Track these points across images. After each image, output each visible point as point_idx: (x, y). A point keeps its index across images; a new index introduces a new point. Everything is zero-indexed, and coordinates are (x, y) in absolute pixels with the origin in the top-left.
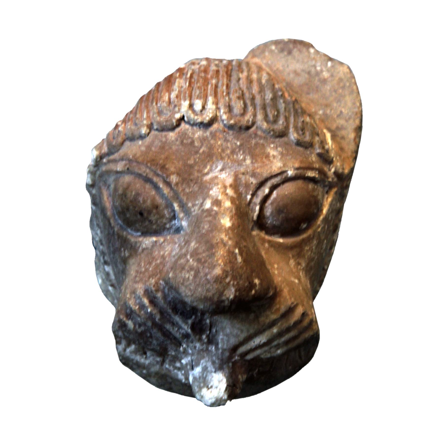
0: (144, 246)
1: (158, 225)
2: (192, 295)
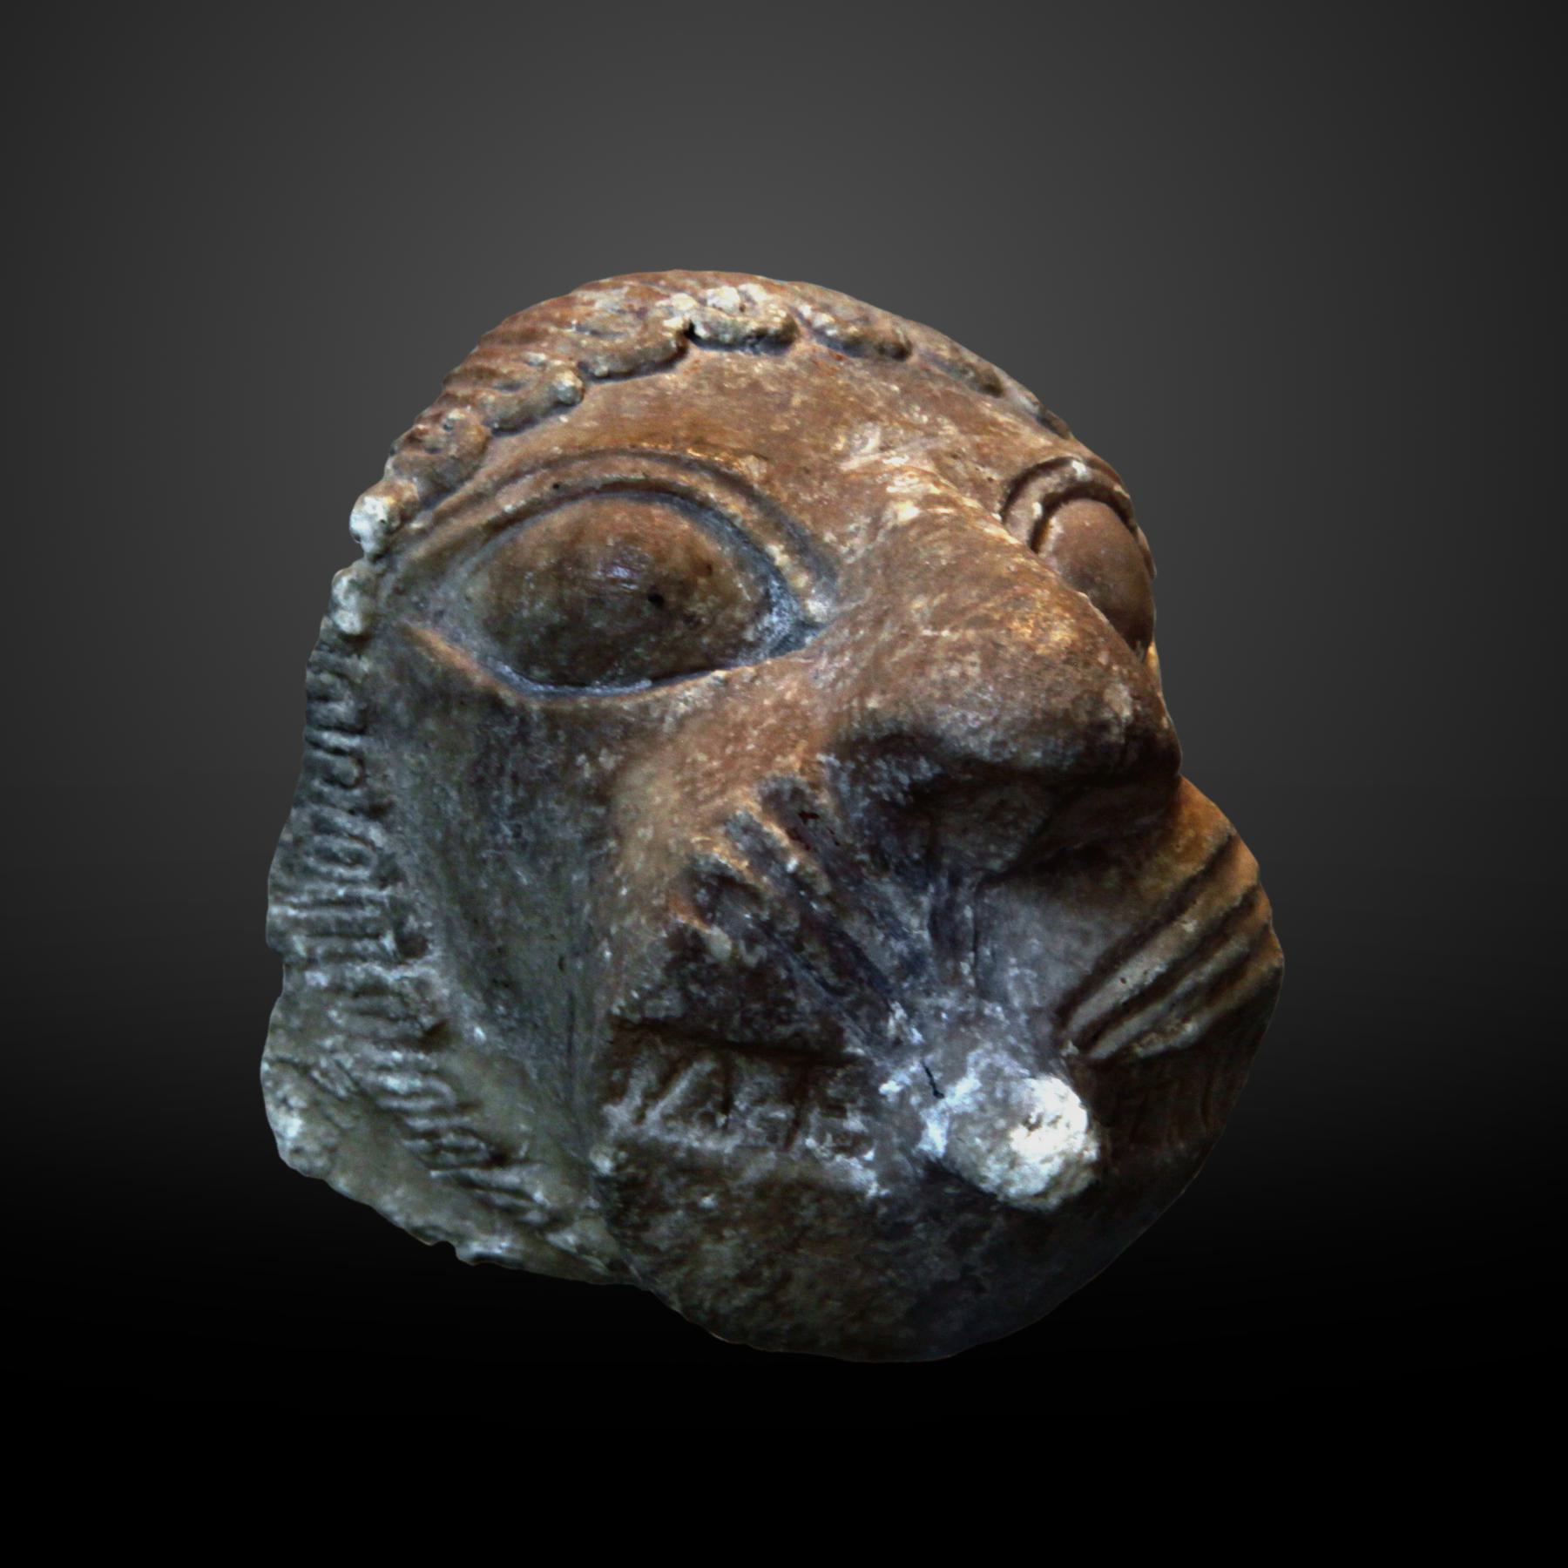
0: (682, 708)
1: (720, 635)
2: (996, 721)
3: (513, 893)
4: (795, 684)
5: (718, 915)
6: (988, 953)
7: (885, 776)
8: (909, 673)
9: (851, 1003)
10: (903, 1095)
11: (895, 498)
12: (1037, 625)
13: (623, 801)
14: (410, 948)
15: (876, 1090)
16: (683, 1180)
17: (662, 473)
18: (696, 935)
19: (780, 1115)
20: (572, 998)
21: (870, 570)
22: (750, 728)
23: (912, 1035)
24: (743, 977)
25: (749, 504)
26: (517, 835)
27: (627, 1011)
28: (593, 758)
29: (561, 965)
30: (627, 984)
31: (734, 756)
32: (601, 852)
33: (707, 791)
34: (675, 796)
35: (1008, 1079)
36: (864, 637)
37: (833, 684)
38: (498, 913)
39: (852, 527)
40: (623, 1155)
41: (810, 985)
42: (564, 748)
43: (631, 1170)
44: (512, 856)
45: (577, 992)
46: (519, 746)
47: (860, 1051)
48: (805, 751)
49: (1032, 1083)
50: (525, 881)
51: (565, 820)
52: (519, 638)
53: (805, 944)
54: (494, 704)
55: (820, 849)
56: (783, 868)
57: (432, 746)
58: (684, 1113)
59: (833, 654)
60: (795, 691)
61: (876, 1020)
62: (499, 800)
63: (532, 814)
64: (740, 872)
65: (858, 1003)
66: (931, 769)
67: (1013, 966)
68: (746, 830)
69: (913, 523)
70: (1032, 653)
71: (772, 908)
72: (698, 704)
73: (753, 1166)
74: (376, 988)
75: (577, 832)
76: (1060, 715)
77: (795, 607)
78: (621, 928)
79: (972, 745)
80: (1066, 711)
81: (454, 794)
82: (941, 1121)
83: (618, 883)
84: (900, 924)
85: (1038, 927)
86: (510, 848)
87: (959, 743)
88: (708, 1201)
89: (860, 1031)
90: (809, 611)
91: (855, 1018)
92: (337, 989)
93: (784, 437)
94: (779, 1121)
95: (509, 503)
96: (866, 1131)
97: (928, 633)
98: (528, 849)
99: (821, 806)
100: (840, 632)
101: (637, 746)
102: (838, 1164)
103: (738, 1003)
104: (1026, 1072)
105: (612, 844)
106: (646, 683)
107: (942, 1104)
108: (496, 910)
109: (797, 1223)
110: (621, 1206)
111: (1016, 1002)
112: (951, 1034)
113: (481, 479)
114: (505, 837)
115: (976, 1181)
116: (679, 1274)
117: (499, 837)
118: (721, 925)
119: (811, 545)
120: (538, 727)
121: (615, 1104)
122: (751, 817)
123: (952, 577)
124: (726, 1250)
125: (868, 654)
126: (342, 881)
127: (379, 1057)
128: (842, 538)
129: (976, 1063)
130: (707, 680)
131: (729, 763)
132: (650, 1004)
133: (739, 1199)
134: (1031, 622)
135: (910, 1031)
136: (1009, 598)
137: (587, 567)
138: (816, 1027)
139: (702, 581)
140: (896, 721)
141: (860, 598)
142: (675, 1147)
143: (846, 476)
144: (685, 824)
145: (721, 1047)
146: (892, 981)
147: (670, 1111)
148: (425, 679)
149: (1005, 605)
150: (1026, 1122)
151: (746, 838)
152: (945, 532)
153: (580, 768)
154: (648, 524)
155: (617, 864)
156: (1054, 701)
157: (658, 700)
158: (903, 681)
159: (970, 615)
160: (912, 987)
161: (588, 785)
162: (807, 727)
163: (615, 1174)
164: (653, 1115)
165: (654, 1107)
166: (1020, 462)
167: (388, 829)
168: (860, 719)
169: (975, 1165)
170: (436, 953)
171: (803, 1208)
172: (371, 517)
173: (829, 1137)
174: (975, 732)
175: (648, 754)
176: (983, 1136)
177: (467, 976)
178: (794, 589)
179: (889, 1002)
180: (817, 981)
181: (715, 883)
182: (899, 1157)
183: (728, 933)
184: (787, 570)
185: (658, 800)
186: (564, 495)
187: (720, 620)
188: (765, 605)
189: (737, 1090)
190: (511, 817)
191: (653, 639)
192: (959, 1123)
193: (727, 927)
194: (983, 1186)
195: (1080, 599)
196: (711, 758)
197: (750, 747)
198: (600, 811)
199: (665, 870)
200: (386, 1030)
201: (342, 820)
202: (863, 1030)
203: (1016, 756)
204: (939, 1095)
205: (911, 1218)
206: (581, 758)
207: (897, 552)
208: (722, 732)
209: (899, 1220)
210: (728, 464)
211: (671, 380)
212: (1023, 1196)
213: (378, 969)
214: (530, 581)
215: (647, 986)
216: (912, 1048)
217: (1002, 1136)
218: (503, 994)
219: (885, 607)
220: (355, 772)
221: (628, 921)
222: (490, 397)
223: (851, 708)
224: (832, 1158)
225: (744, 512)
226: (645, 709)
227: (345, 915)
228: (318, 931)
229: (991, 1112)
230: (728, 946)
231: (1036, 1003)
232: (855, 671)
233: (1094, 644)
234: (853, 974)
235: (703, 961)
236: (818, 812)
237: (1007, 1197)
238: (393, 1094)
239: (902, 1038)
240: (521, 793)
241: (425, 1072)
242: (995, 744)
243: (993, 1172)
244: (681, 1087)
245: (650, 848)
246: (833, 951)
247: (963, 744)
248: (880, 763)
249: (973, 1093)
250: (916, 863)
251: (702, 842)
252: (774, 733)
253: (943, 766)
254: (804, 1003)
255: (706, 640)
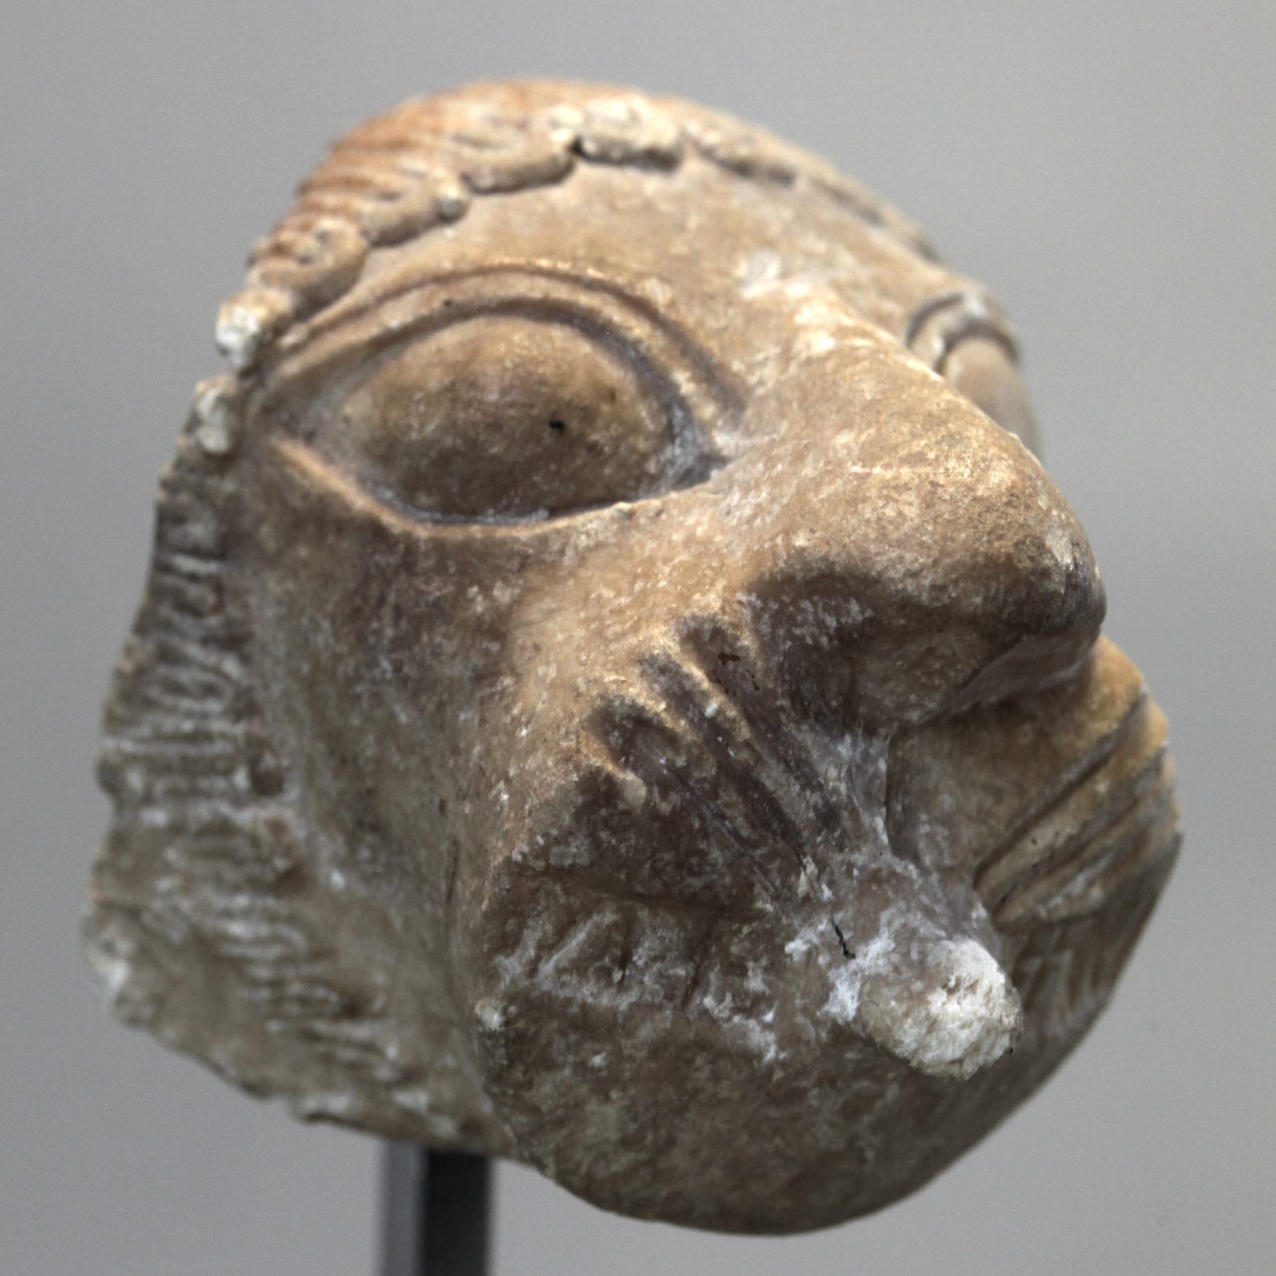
0: (583, 541)
1: (621, 466)
2: (935, 563)
3: (390, 731)
4: (705, 519)
5: (632, 759)
6: (899, 808)
7: (811, 618)
8: (841, 510)
9: (762, 856)
10: (810, 955)
11: (805, 328)
12: (975, 464)
13: (521, 638)
14: (266, 786)
15: (782, 947)
16: (573, 1037)
17: (561, 293)
18: (609, 779)
19: (681, 972)
20: (455, 843)
21: (783, 403)
22: (660, 564)
23: (822, 891)
24: (656, 825)
25: (654, 328)
26: (398, 669)
27: (530, 858)
28: (486, 591)
29: (442, 807)
30: (530, 829)
31: (643, 591)
32: (494, 690)
33: (618, 628)
34: (580, 633)
35: (924, 940)
36: (783, 472)
37: (750, 520)
38: (369, 752)
39: (760, 357)
40: (513, 1009)
41: (723, 836)
42: (454, 579)
43: (521, 1024)
44: (390, 692)
45: (462, 836)
46: (403, 577)
47: (769, 907)
48: (724, 589)
49: (950, 945)
50: (403, 719)
51: (455, 655)
52: (405, 462)
53: (721, 793)
54: (375, 532)
55: (738, 693)
56: (702, 713)
57: (303, 574)
58: (579, 967)
59: (746, 490)
60: (706, 527)
61: (788, 875)
62: (378, 633)
63: (416, 649)
64: (657, 714)
65: (772, 856)
66: (862, 613)
67: (924, 823)
68: (663, 670)
69: (830, 355)
70: (972, 494)
71: (689, 752)
72: (601, 537)
73: (648, 1024)
74: (223, 828)
75: (466, 669)
76: (1003, 559)
77: (700, 439)
78: (522, 770)
79: (910, 589)
80: (1009, 556)
81: (326, 625)
82: (852, 983)
83: (516, 723)
84: (816, 775)
85: (950, 782)
86: (389, 683)
87: (896, 586)
88: (597, 1060)
89: (768, 885)
90: (715, 443)
91: (766, 873)
92: (176, 829)
93: (681, 259)
94: (678, 978)
95: (395, 316)
96: (768, 992)
97: (857, 469)
98: (410, 685)
99: (742, 648)
100: (753, 466)
101: (533, 578)
102: (735, 1025)
103: (649, 853)
104: (942, 933)
105: (507, 681)
106: (543, 513)
107: (853, 965)
108: (369, 747)
109: (689, 1086)
110: (505, 1062)
111: (927, 860)
112: (862, 893)
113: (360, 293)
114: (384, 672)
115: (890, 1044)
116: (561, 1135)
117: (377, 672)
118: (635, 769)
119: (718, 374)
120: (427, 556)
121: (507, 956)
122: (669, 656)
123: (879, 413)
124: (611, 1112)
125: (789, 491)
126: (189, 715)
127: (220, 902)
128: (751, 367)
129: (890, 923)
130: (607, 512)
131: (640, 599)
132: (555, 850)
133: (631, 1059)
134: (969, 462)
135: (820, 887)
136: (943, 437)
137: (484, 389)
138: (728, 880)
139: (605, 408)
140: (827, 560)
141: (774, 431)
142: (568, 1002)
143: (749, 305)
144: (595, 662)
145: (628, 896)
146: (805, 834)
147: (565, 964)
148: (296, 502)
149: (938, 443)
150: (945, 986)
151: (662, 679)
152: (866, 364)
153: (472, 600)
154: (548, 346)
155: (514, 702)
156: (996, 544)
157: (558, 532)
158: (834, 519)
159: (903, 452)
160: (826, 841)
161: (479, 619)
162: (723, 565)
163: (503, 1029)
164: (547, 968)
165: (547, 961)
166: (920, 298)
167: (245, 660)
168: (785, 557)
169: (889, 1029)
170: (293, 792)
171: (697, 1069)
172: (241, 330)
173: (729, 997)
174: (914, 575)
175: (547, 588)
176: (899, 999)
177: (328, 819)
178: (701, 420)
179: (802, 857)
180: (729, 832)
181: (630, 726)
182: (800, 1019)
183: (643, 778)
184: (694, 400)
185: (560, 637)
186: (456, 313)
187: (623, 449)
188: (669, 435)
189: (637, 944)
190: (392, 650)
191: (553, 467)
192: (872, 985)
193: (641, 772)
194: (898, 1051)
195: (1013, 439)
196: (619, 594)
197: (662, 584)
198: (495, 647)
199: (575, 710)
200: (230, 874)
201: (194, 651)
202: (773, 884)
203: (955, 602)
204: (849, 955)
205: (805, 1083)
206: (474, 590)
207: (814, 385)
208: (628, 567)
209: (794, 1085)
210: (631, 285)
211: (561, 196)
212: (939, 1062)
213: (225, 809)
214: (419, 401)
215: (555, 832)
216: (822, 905)
217: (920, 999)
218: (370, 838)
219: (804, 442)
220: (211, 599)
221: (531, 764)
222: (367, 206)
223: (776, 545)
224: (729, 1019)
225: (650, 337)
226: (544, 540)
227: (193, 751)
228: (156, 767)
229: (906, 974)
230: (643, 792)
231: (948, 862)
232: (776, 508)
233: (1034, 487)
234: (767, 825)
235: (616, 806)
236: (739, 654)
237: (921, 1063)
238: (236, 940)
239: (812, 895)
240: (404, 624)
241: (272, 918)
242: (934, 587)
243: (908, 1037)
244: (578, 938)
245: (553, 686)
246: (747, 799)
247: (900, 586)
248: (806, 604)
249: (886, 954)
250: (835, 711)
251: (616, 682)
252: (688, 569)
253: (874, 609)
254: (716, 855)
255: (607, 471)
